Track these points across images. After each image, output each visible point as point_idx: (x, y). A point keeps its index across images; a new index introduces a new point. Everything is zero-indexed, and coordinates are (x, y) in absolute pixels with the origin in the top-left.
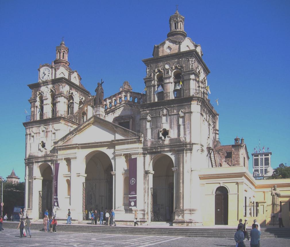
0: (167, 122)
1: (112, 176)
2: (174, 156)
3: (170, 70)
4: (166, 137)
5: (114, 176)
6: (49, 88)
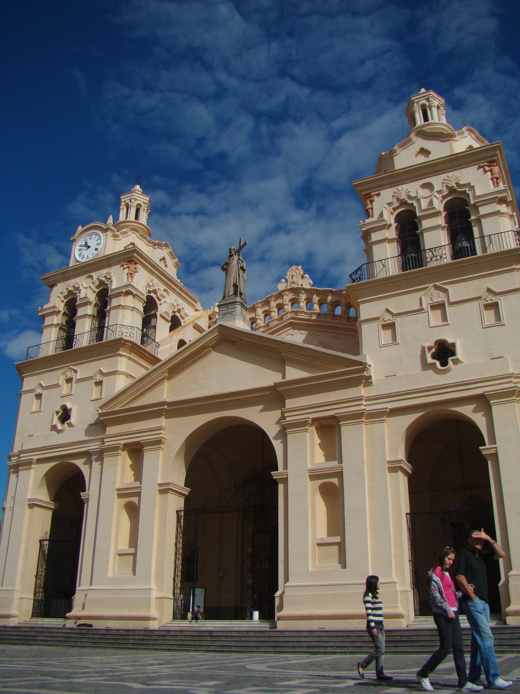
0: (445, 323)
1: (275, 484)
2: (483, 413)
3: (434, 199)
4: (450, 363)
5: (281, 487)
6: (95, 277)
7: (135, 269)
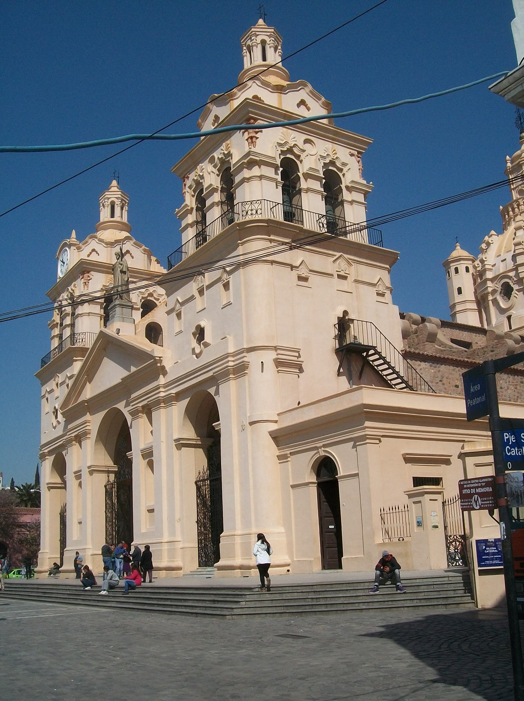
7: (89, 277)
